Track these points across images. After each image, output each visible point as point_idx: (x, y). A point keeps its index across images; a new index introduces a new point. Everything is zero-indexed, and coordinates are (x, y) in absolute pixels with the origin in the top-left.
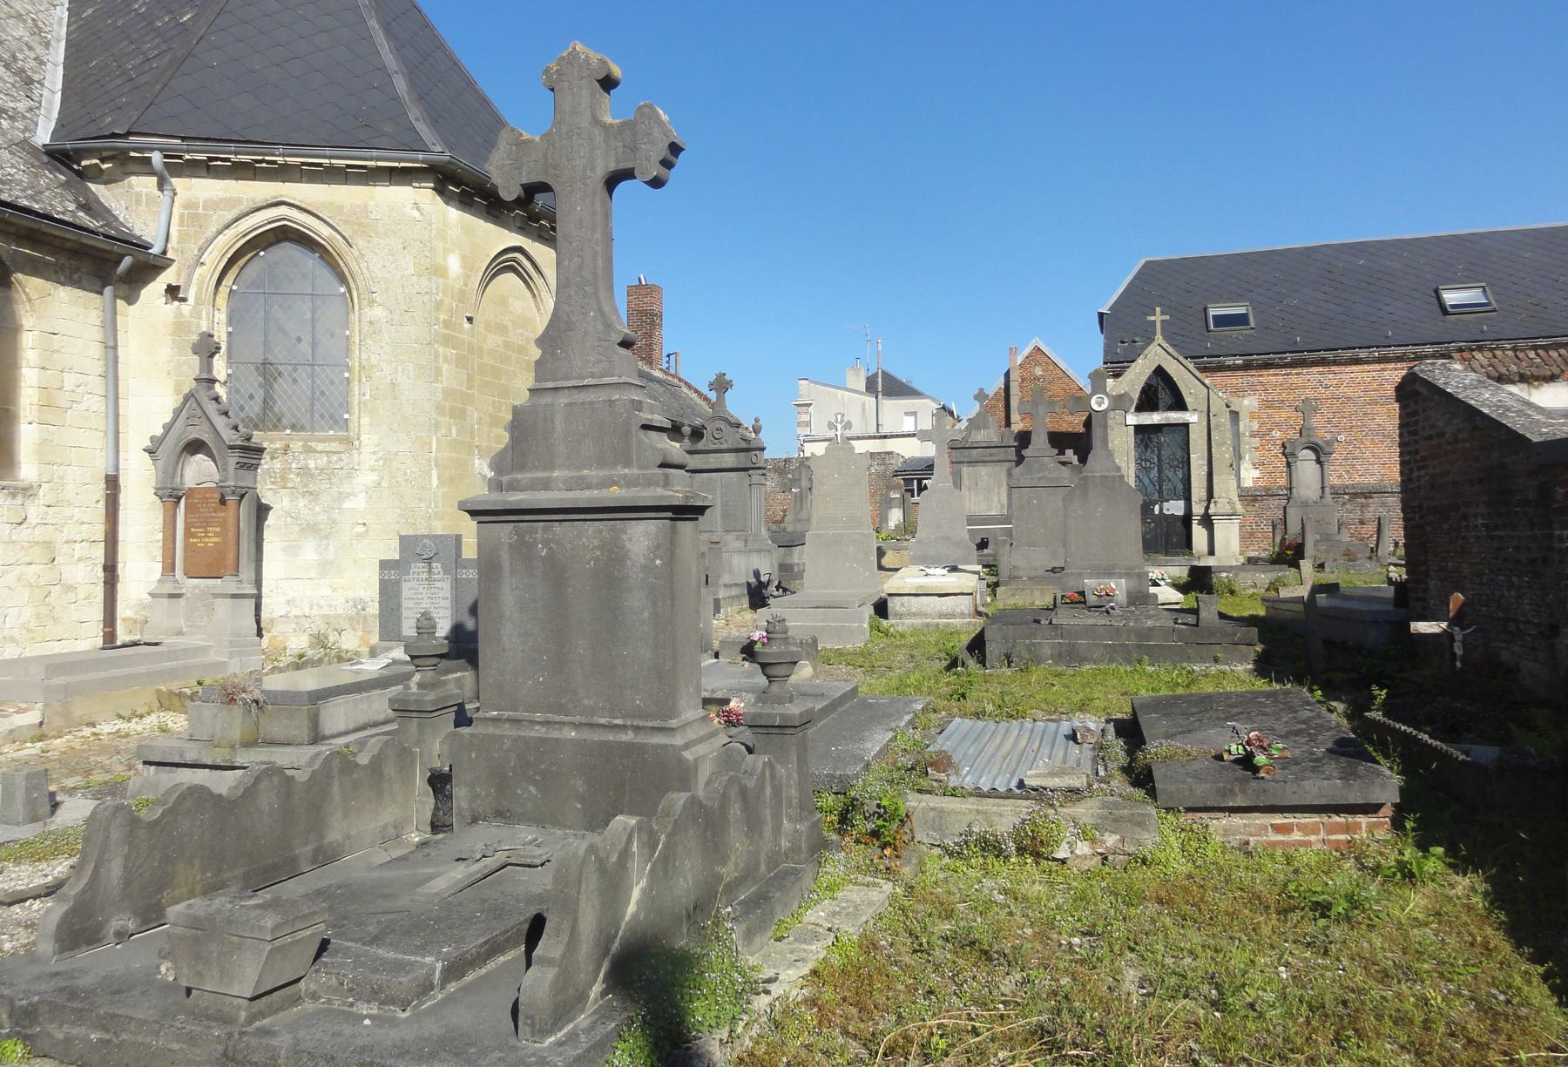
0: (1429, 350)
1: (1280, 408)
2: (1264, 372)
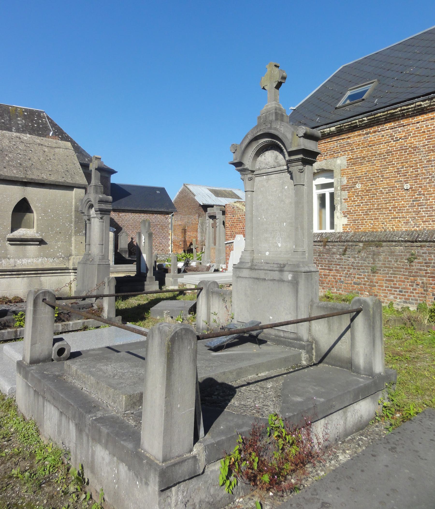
1: (361, 164)
2: (351, 135)
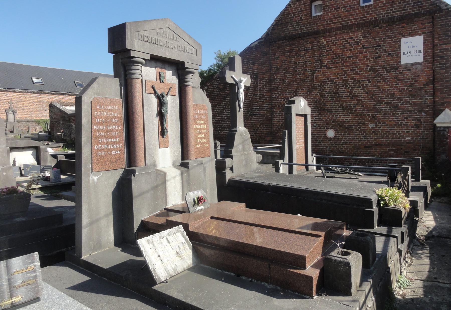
0: (31, 91)
